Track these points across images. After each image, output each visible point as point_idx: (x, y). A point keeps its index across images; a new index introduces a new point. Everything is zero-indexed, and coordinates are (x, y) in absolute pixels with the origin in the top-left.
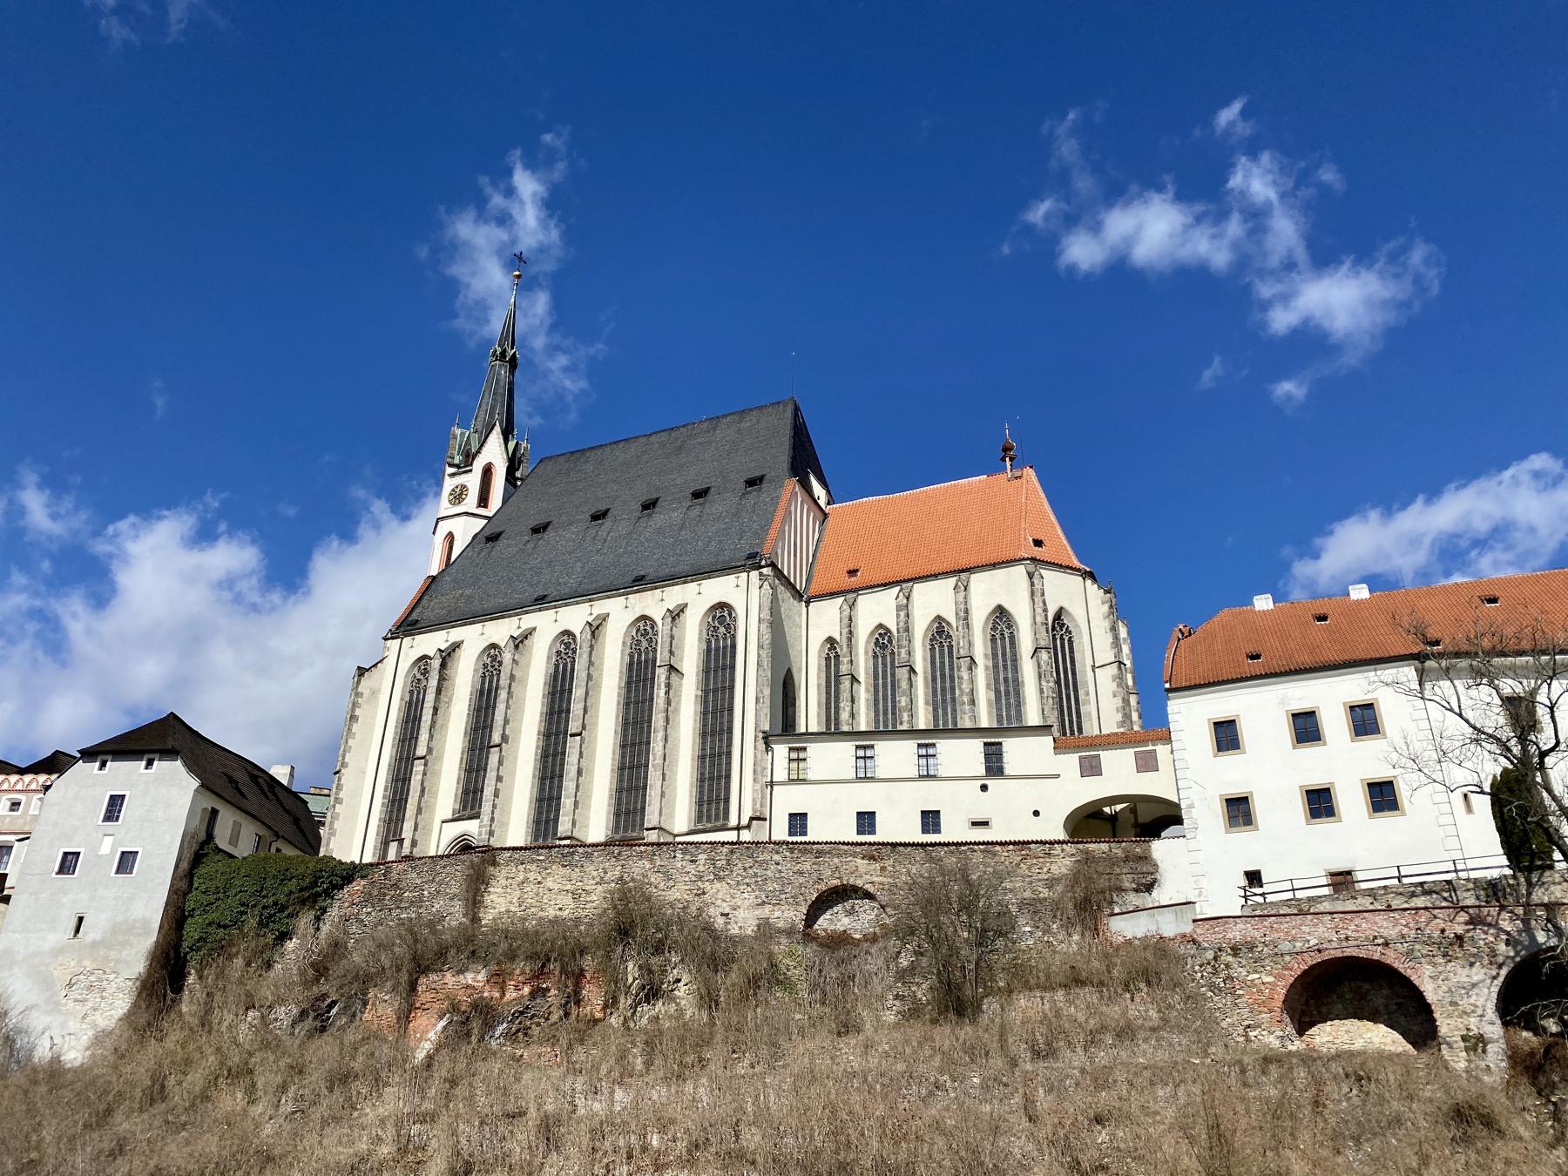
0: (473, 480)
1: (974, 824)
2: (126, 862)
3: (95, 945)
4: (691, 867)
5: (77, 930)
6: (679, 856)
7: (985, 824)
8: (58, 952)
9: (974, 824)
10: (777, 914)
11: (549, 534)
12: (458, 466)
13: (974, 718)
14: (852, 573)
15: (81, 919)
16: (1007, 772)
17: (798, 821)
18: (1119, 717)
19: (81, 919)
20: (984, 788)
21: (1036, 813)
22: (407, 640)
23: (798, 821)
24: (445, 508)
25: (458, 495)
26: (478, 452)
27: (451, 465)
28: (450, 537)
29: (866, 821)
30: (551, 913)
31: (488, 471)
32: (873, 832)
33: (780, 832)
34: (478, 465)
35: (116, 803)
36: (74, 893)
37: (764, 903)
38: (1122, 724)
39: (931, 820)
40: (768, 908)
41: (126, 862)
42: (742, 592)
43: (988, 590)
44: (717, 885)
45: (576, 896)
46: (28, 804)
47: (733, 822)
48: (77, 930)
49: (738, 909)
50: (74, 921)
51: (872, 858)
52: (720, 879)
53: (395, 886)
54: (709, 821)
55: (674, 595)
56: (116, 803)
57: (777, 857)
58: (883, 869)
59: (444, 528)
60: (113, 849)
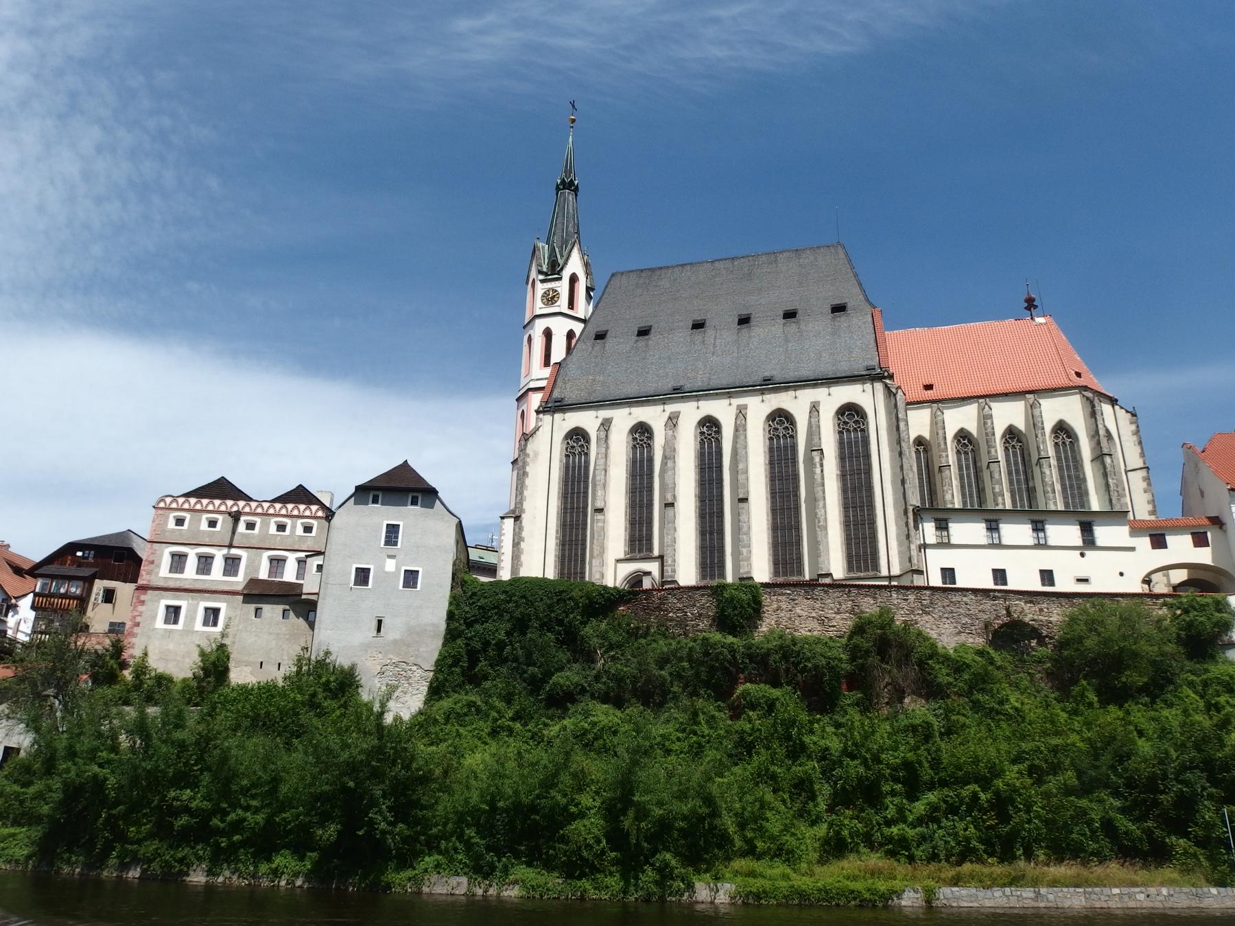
0: (563, 287)
1: (1079, 580)
2: (411, 578)
3: (395, 642)
4: (904, 604)
5: (379, 630)
6: (894, 595)
7: (1086, 580)
8: (365, 647)
9: (1079, 580)
10: (971, 640)
11: (653, 337)
12: (546, 274)
13: (1004, 504)
14: (929, 387)
15: (380, 622)
16: (1099, 543)
17: (948, 574)
18: (1150, 507)
19: (380, 622)
20: (1082, 555)
21: (1121, 574)
22: (558, 416)
23: (948, 574)
24: (540, 308)
25: (551, 298)
26: (566, 263)
27: (540, 272)
28: (548, 334)
29: (1000, 575)
30: (804, 633)
31: (573, 279)
32: (1005, 584)
33: (936, 580)
34: (566, 274)
35: (393, 530)
36: (370, 601)
37: (959, 633)
38: (1153, 512)
39: (1047, 576)
40: (963, 637)
41: (411, 578)
42: (864, 395)
43: (1054, 410)
44: (926, 618)
45: (821, 621)
46: (294, 527)
47: (884, 572)
48: (379, 630)
49: (947, 634)
50: (375, 624)
51: (1031, 602)
52: (928, 613)
53: (659, 608)
54: (785, 574)
55: (807, 396)
56: (393, 530)
57: (965, 599)
58: (1041, 610)
59: (540, 325)
60: (398, 568)
